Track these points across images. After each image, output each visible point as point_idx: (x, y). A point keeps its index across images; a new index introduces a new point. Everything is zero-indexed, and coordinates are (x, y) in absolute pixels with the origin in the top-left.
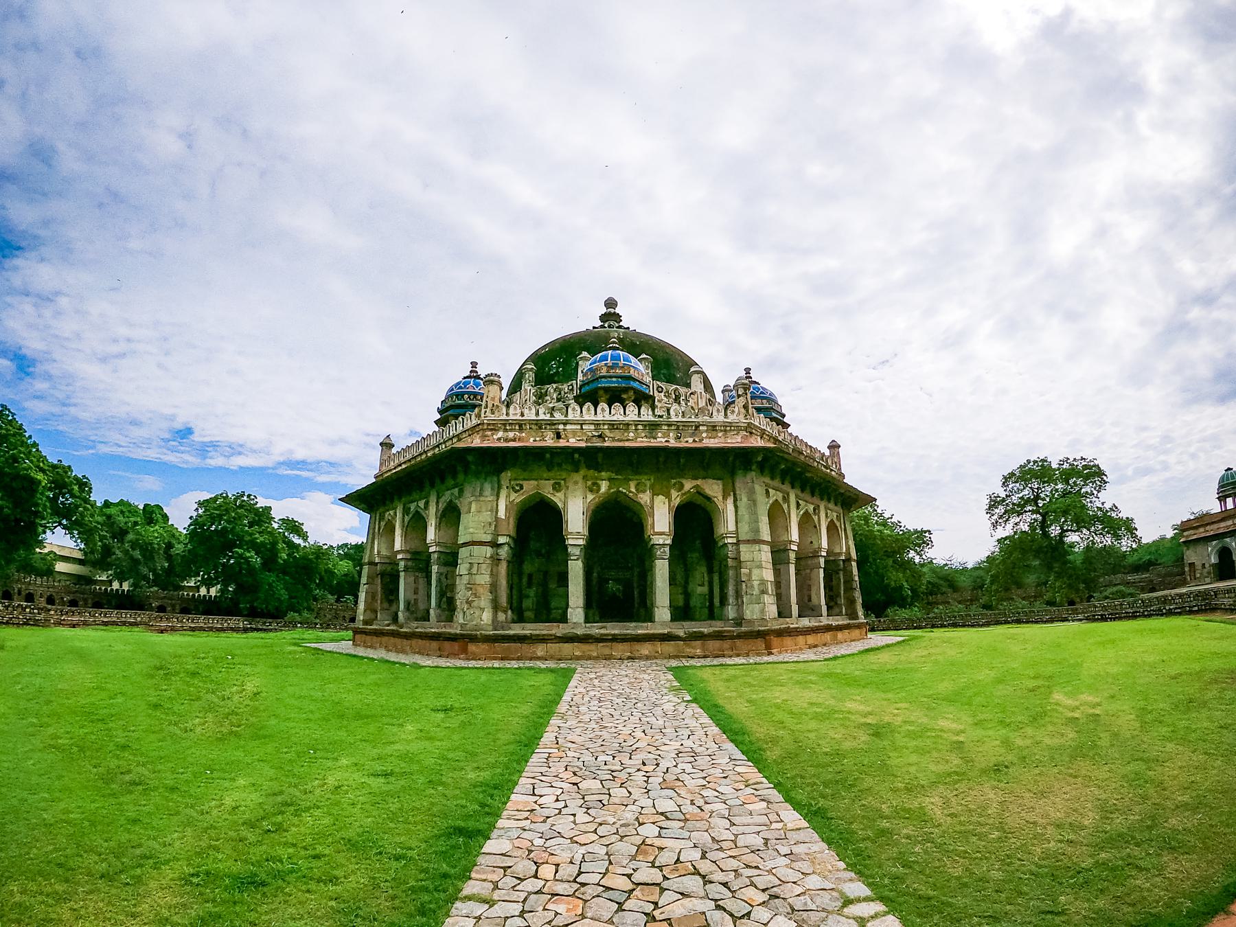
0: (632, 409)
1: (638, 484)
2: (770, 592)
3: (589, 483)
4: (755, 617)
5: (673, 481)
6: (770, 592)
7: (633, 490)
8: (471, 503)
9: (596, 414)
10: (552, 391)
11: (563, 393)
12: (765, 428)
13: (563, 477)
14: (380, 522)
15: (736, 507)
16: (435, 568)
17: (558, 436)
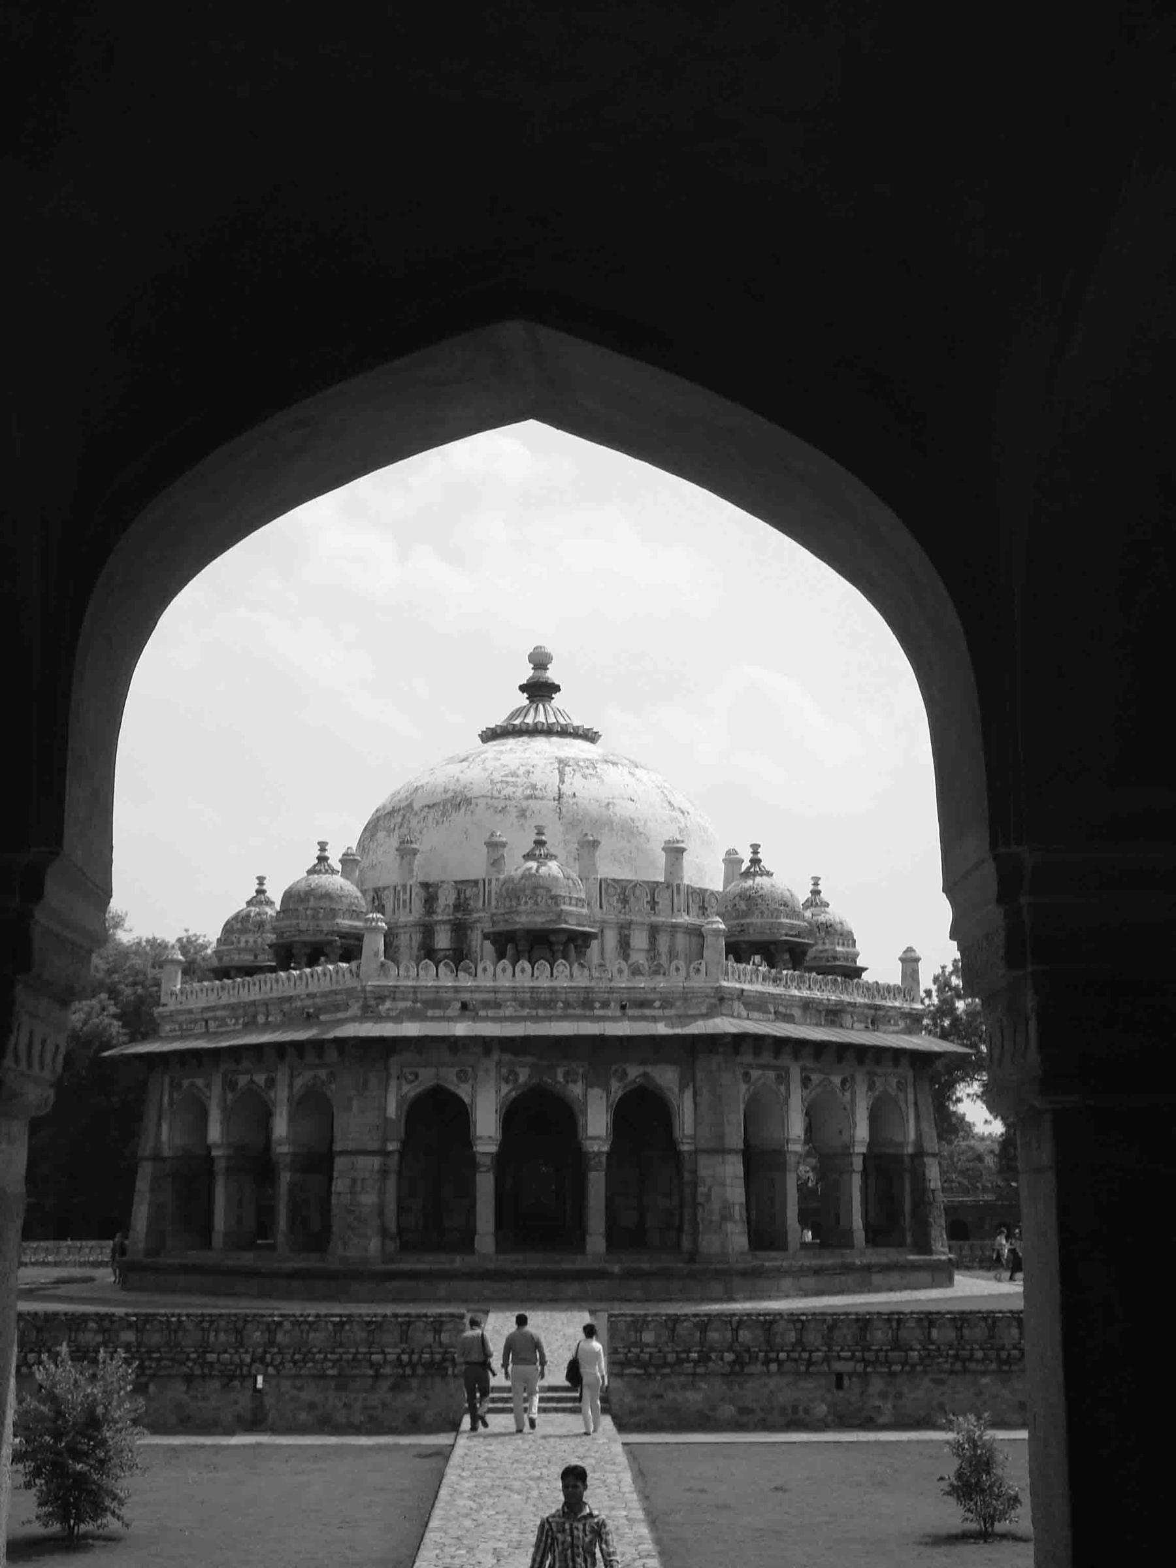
2: (737, 1216)
3: (504, 1071)
6: (737, 1216)
7: (562, 1080)
8: (350, 1100)
9: (514, 975)
10: (447, 892)
11: (462, 896)
12: (746, 987)
15: (696, 1104)
16: (285, 1177)
17: (464, 1006)
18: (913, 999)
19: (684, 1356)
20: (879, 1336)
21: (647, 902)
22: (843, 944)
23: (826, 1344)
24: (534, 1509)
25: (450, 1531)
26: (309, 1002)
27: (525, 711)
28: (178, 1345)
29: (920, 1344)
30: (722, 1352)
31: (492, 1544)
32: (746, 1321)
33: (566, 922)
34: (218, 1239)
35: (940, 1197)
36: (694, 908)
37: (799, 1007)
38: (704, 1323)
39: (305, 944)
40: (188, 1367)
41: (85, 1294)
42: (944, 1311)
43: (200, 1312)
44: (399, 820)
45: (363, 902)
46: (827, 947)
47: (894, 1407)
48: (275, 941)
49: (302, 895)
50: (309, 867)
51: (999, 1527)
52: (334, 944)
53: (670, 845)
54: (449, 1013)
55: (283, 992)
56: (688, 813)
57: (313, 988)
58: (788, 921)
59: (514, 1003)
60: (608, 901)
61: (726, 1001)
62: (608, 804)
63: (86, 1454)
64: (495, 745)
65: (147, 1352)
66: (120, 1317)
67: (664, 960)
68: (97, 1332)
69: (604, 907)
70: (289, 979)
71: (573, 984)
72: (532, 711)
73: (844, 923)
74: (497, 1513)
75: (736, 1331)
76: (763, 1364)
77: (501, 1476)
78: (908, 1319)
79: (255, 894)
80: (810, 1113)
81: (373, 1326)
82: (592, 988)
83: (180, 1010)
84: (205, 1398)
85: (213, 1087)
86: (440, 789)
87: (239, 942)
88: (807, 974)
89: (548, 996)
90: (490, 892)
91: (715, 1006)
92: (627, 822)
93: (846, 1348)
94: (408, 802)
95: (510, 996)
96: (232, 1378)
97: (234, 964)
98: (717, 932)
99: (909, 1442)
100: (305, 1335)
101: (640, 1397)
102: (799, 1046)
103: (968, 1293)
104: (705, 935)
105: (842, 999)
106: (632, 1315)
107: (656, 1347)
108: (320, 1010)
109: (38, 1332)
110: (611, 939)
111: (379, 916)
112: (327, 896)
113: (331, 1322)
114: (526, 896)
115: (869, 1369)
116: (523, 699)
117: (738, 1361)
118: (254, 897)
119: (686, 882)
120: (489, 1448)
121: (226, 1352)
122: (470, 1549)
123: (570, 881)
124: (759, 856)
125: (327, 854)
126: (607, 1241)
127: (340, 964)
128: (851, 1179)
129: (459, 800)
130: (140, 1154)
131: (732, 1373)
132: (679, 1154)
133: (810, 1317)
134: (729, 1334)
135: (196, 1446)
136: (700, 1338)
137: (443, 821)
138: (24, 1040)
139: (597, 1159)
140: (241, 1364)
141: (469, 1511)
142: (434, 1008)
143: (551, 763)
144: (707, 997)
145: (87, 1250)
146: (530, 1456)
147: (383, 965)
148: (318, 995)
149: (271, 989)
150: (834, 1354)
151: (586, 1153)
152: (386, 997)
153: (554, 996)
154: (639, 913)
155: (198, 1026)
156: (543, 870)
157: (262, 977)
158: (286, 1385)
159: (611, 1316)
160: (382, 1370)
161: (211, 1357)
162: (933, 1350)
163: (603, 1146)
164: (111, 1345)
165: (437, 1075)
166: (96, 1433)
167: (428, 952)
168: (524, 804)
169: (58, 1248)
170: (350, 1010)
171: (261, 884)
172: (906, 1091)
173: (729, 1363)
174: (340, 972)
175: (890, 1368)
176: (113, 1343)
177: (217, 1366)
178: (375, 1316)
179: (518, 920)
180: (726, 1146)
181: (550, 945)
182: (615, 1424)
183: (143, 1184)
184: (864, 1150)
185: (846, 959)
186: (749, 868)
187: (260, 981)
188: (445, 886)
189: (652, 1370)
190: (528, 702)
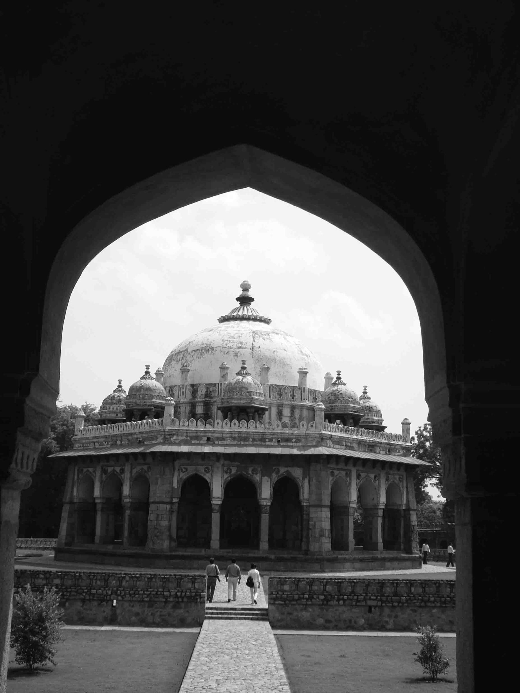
0: (252, 423)
1: (253, 470)
2: (327, 535)
3: (225, 468)
4: (316, 550)
5: (274, 468)
6: (327, 535)
8: (157, 479)
9: (231, 426)
10: (202, 388)
12: (333, 434)
13: (211, 465)
14: (78, 476)
16: (128, 512)
17: (209, 439)
18: (407, 441)
19: (302, 596)
20: (388, 590)
21: (290, 395)
22: (377, 416)
23: (365, 593)
24: (235, 662)
25: (197, 671)
26: (139, 436)
27: (238, 309)
28: (79, 586)
29: (406, 594)
30: (319, 595)
31: (216, 677)
32: (330, 581)
33: (255, 404)
34: (97, 539)
35: (416, 528)
36: (311, 398)
37: (357, 443)
38: (311, 582)
39: (139, 410)
40: (83, 595)
41: (39, 562)
42: (417, 580)
43: (89, 571)
44: (182, 356)
45: (165, 392)
46: (370, 417)
47: (394, 621)
48: (125, 408)
49: (138, 387)
50: (141, 376)
51: (439, 676)
52: (152, 411)
53: (301, 370)
54: (202, 442)
55: (129, 431)
56: (310, 356)
57: (142, 429)
58: (352, 405)
59: (230, 439)
60: (273, 395)
61: (324, 440)
62: (274, 351)
63: (38, 633)
64: (224, 324)
65: (65, 589)
66: (54, 573)
67: (297, 421)
68: (43, 579)
69: (271, 398)
70: (131, 425)
71: (257, 431)
72: (241, 309)
73: (377, 407)
74: (218, 663)
75: (325, 586)
76: (336, 601)
77: (220, 647)
78: (401, 583)
79: (117, 387)
80: (360, 491)
81: (166, 580)
82: (265, 433)
83: (83, 438)
84: (91, 610)
85: (97, 473)
86: (200, 343)
87: (110, 408)
88: (360, 429)
89: (246, 435)
90: (221, 389)
91: (319, 441)
92: (282, 359)
93: (373, 595)
94: (186, 348)
95: (229, 435)
96: (102, 601)
97: (107, 418)
98: (321, 409)
99: (400, 637)
100: (135, 582)
101: (283, 614)
102: (356, 460)
103: (428, 572)
104: (315, 410)
105: (376, 440)
106: (280, 578)
107: (290, 592)
108: (145, 439)
109: (17, 579)
110: (274, 411)
111: (172, 398)
112: (149, 389)
113: (148, 578)
114: (237, 391)
115: (384, 605)
116: (237, 304)
117: (326, 600)
118: (116, 389)
119: (308, 387)
120: (215, 635)
121: (100, 589)
122: (206, 680)
123: (257, 385)
124: (341, 376)
125: (149, 370)
126: (269, 545)
127: (154, 419)
128: (377, 520)
129: (208, 348)
130: (64, 500)
131: (323, 605)
132: (301, 507)
133: (358, 581)
134: (322, 587)
135: (86, 630)
136: (309, 590)
137: (201, 358)
138: (20, 456)
139: (265, 508)
140: (107, 595)
141: (206, 663)
142: (195, 440)
143: (249, 333)
144: (316, 438)
145: (39, 542)
146: (233, 639)
147: (173, 420)
148: (144, 433)
149: (124, 430)
150: (369, 597)
151: (261, 505)
152: (175, 434)
153: (248, 436)
154: (287, 401)
155: (91, 445)
156: (245, 380)
157: (120, 424)
158: (126, 604)
159: (270, 578)
160: (169, 599)
161: (94, 591)
162: (412, 597)
163: (268, 502)
164: (49, 585)
165: (196, 469)
166: (42, 624)
167: (193, 415)
168: (238, 350)
169: (27, 541)
170: (158, 440)
171: (120, 383)
172: (403, 482)
173: (322, 600)
174: (154, 423)
175: (392, 604)
176: (50, 584)
177: (96, 595)
178: (166, 575)
179: (233, 401)
180: (324, 504)
181: (247, 414)
182: (271, 626)
183: (65, 514)
184: (383, 507)
185: (378, 422)
186: (336, 381)
187: (118, 426)
188: (201, 386)
189: (287, 602)
190: (240, 305)
